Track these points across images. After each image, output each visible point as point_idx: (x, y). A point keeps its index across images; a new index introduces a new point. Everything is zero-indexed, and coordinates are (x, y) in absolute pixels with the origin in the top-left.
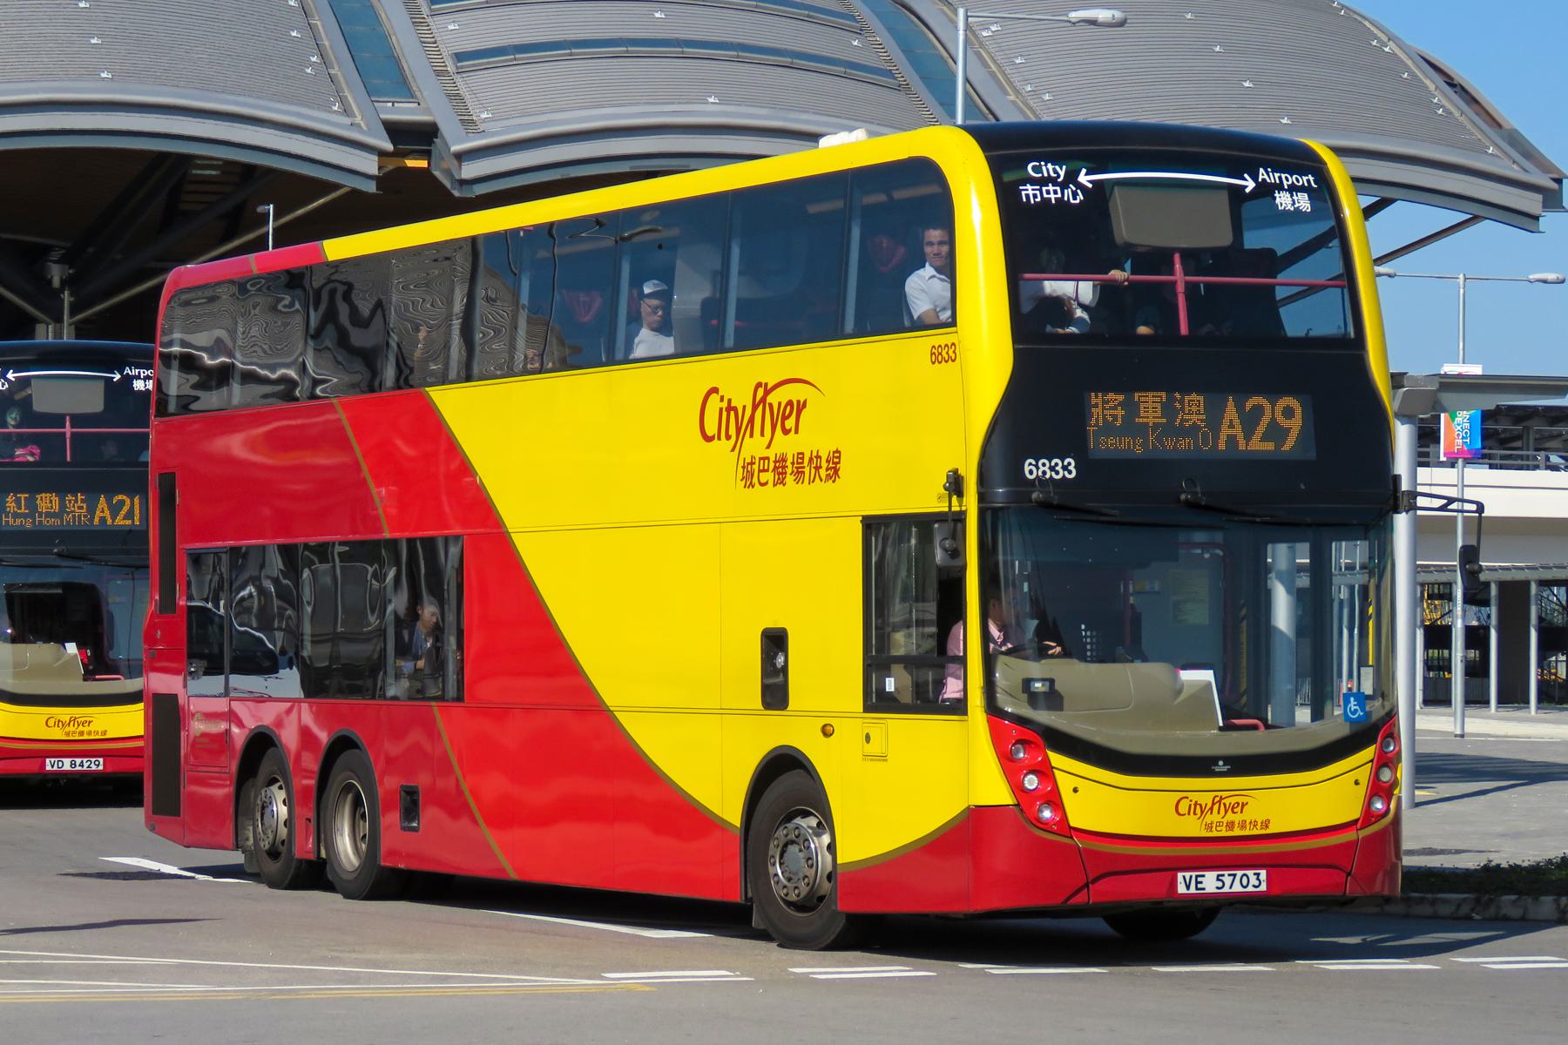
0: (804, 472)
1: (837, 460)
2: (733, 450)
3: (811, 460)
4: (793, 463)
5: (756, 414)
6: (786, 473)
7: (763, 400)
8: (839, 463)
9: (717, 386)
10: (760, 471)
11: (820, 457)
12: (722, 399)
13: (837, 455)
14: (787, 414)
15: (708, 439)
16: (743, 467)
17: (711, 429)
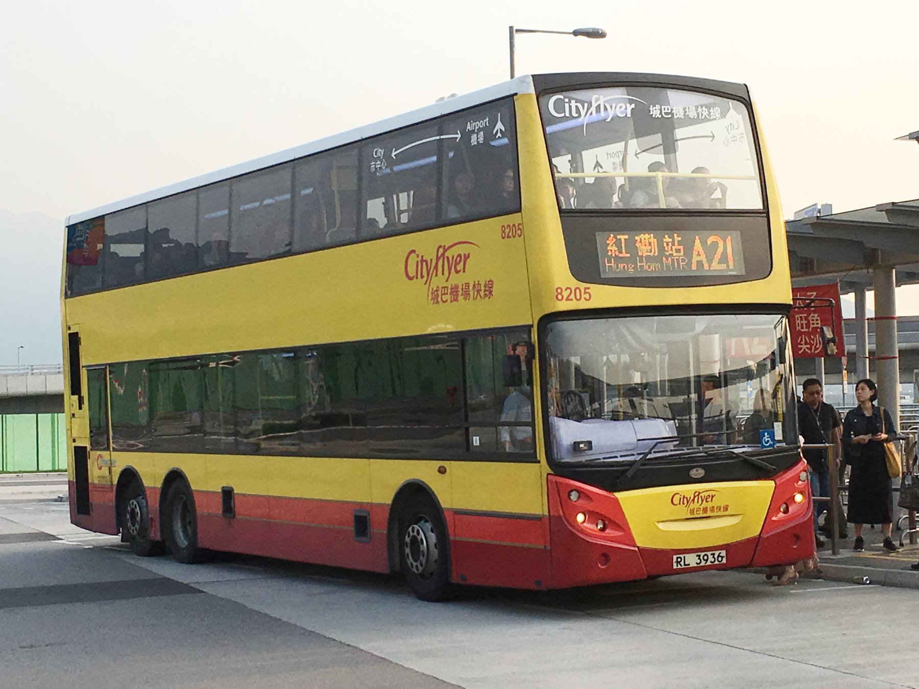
0: (469, 294)
1: (490, 286)
2: (425, 284)
3: (474, 286)
4: (462, 289)
5: (439, 263)
6: (458, 295)
7: (443, 254)
8: (492, 287)
9: (414, 249)
10: (442, 295)
11: (480, 285)
12: (418, 256)
13: (490, 283)
14: (458, 261)
15: (410, 278)
16: (432, 293)
17: (412, 272)
